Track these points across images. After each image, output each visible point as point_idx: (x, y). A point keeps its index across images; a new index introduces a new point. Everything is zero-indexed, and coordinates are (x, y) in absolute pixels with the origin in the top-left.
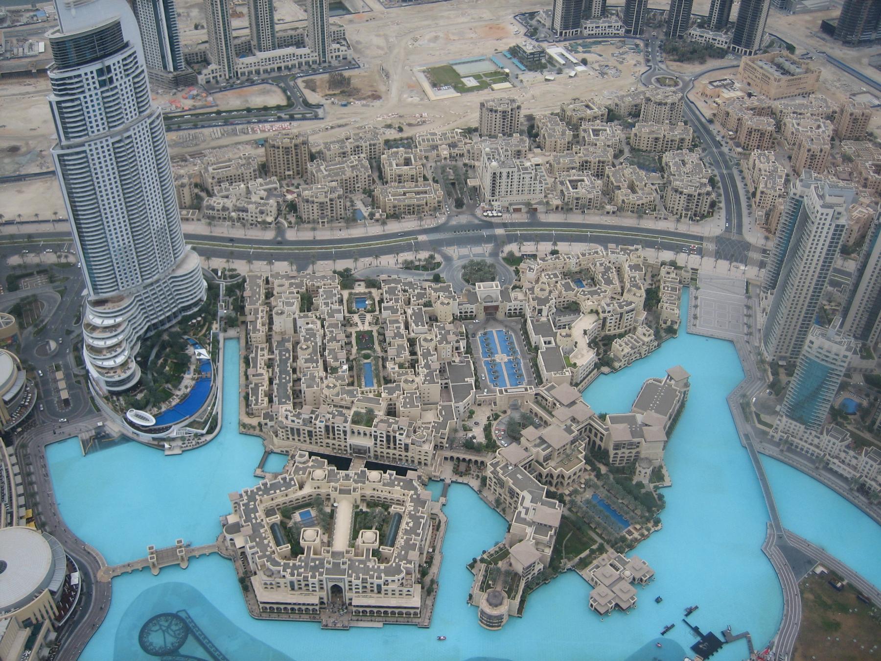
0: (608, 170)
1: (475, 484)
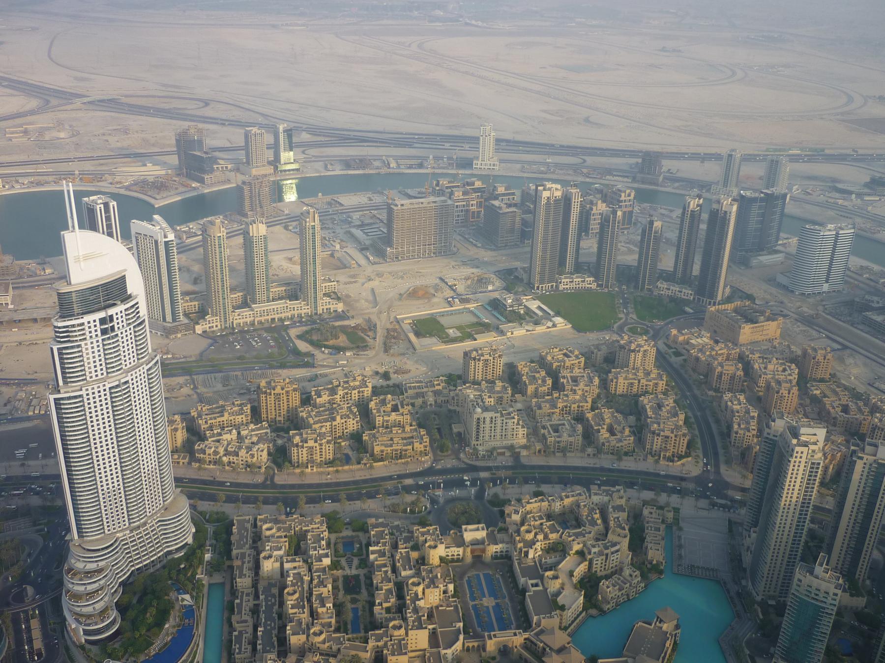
0: (589, 416)
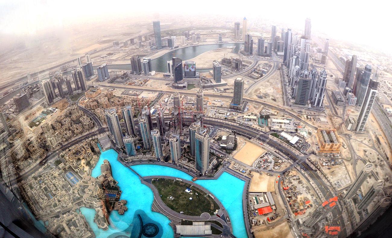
0: (71, 128)
1: (84, 205)
